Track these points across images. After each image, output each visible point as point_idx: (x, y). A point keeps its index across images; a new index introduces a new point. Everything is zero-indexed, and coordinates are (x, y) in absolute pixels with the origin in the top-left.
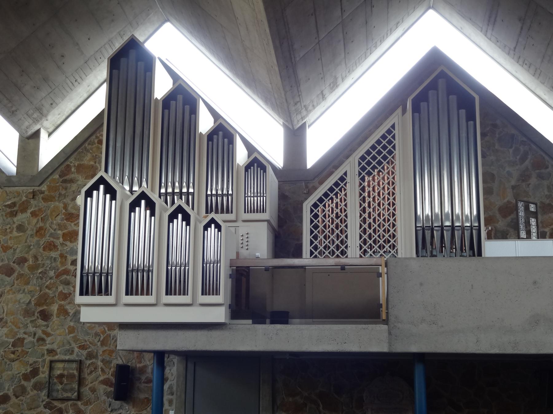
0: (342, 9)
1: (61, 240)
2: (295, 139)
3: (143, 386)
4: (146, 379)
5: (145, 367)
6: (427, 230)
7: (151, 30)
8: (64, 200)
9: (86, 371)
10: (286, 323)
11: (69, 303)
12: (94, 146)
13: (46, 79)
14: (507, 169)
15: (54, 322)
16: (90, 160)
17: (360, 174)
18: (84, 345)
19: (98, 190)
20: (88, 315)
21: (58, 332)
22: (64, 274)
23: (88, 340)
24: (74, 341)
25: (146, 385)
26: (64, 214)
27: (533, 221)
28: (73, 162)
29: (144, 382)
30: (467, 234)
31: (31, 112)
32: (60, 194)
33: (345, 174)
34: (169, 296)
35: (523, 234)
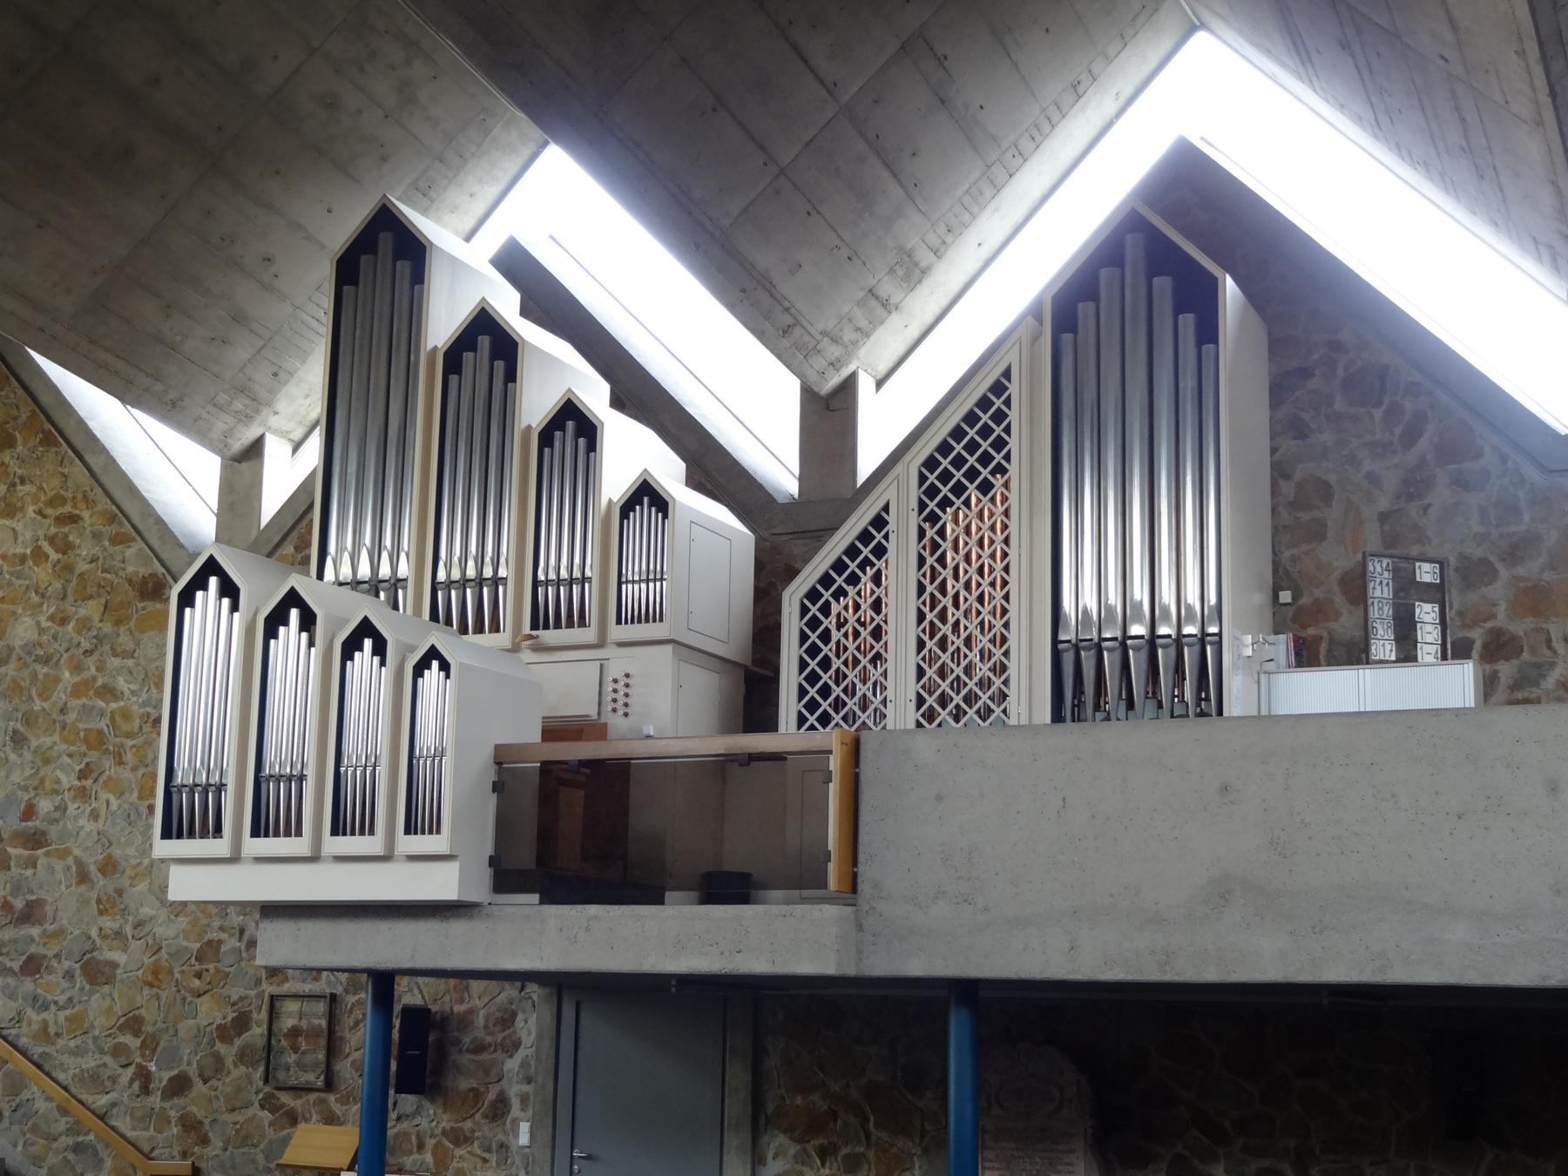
0: (822, 82)
2: (828, 416)
3: (465, 1059)
5: (471, 1012)
6: (1084, 648)
7: (512, 167)
10: (744, 899)
13: (239, 318)
14: (1368, 466)
17: (922, 506)
20: (187, 885)
27: (1427, 613)
29: (468, 1051)
30: (1136, 662)
31: (222, 398)
33: (886, 508)
35: (1383, 647)
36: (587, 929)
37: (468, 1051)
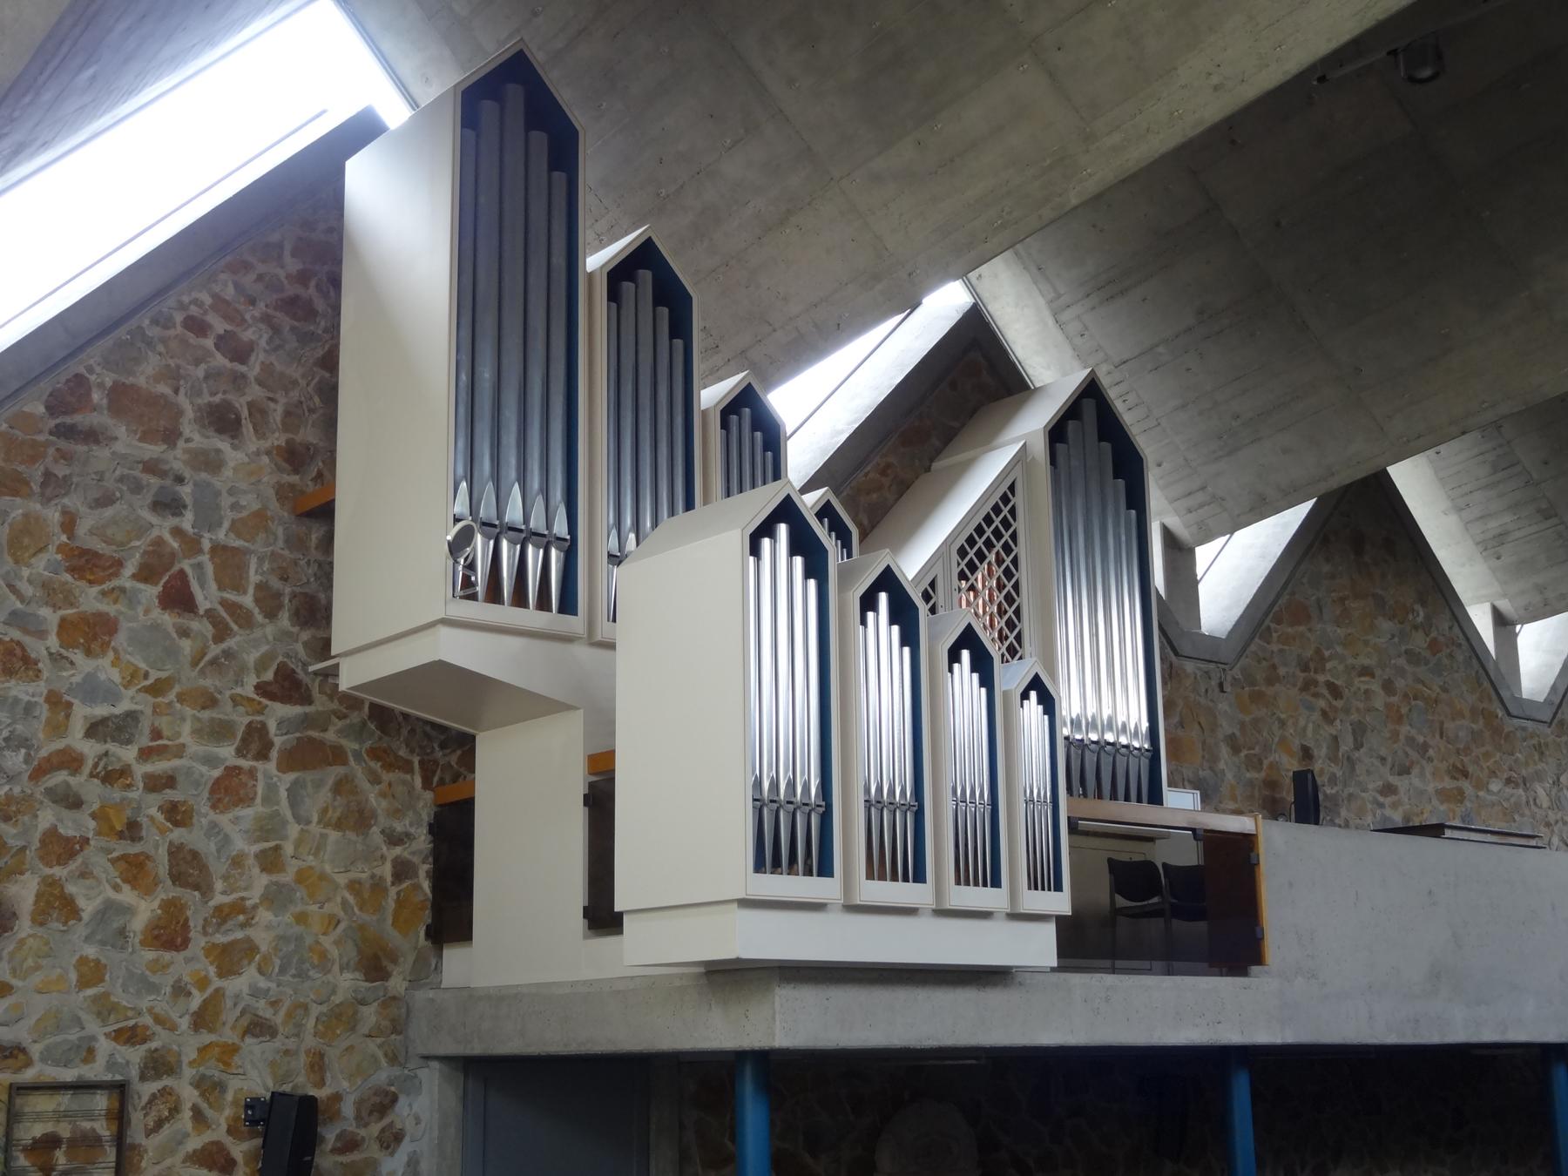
1: (53, 642)
4: (339, 1137)
5: (337, 1098)
8: (66, 501)
9: (137, 1119)
11: (84, 875)
12: (172, 332)
15: (22, 942)
16: (158, 378)
18: (135, 1027)
19: (772, 534)
21: (37, 979)
22: (60, 767)
23: (150, 1010)
24: (99, 1014)
25: (341, 1159)
26: (60, 549)
28: (98, 369)
29: (334, 1151)
32: (48, 475)
34: (963, 888)
36: (1107, 1000)
37: (334, 1151)
